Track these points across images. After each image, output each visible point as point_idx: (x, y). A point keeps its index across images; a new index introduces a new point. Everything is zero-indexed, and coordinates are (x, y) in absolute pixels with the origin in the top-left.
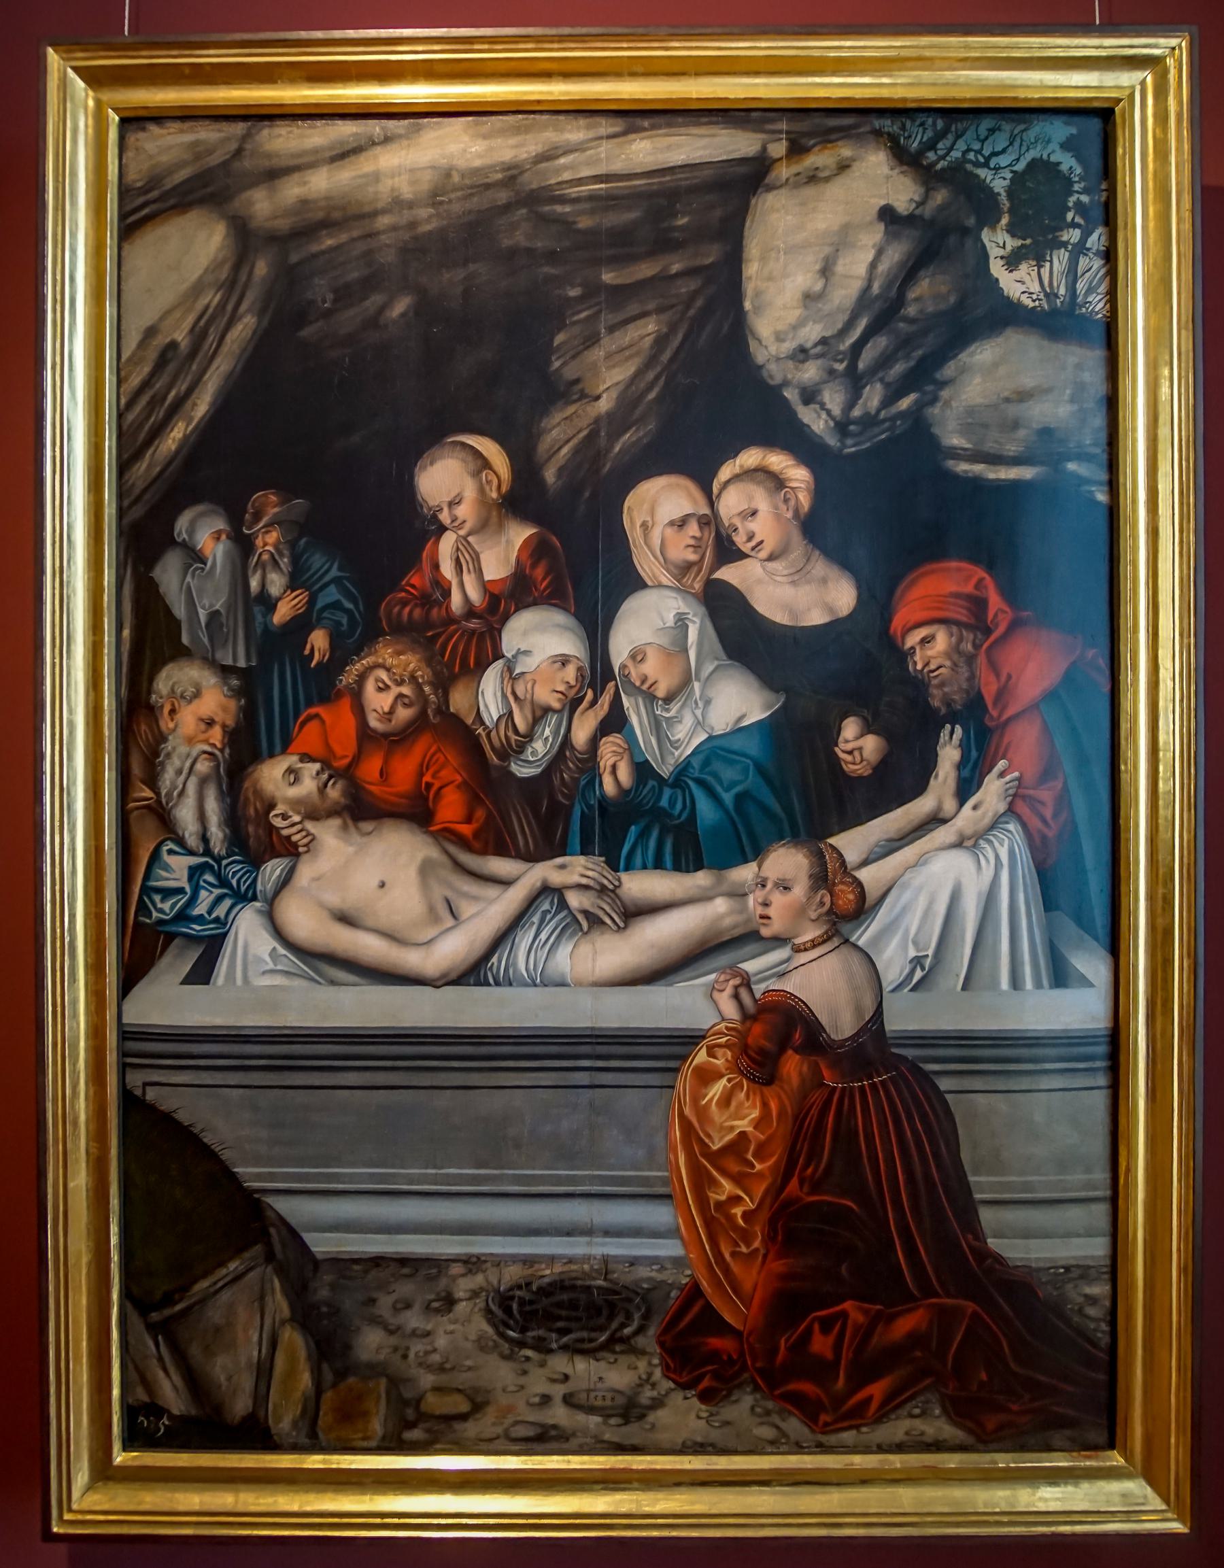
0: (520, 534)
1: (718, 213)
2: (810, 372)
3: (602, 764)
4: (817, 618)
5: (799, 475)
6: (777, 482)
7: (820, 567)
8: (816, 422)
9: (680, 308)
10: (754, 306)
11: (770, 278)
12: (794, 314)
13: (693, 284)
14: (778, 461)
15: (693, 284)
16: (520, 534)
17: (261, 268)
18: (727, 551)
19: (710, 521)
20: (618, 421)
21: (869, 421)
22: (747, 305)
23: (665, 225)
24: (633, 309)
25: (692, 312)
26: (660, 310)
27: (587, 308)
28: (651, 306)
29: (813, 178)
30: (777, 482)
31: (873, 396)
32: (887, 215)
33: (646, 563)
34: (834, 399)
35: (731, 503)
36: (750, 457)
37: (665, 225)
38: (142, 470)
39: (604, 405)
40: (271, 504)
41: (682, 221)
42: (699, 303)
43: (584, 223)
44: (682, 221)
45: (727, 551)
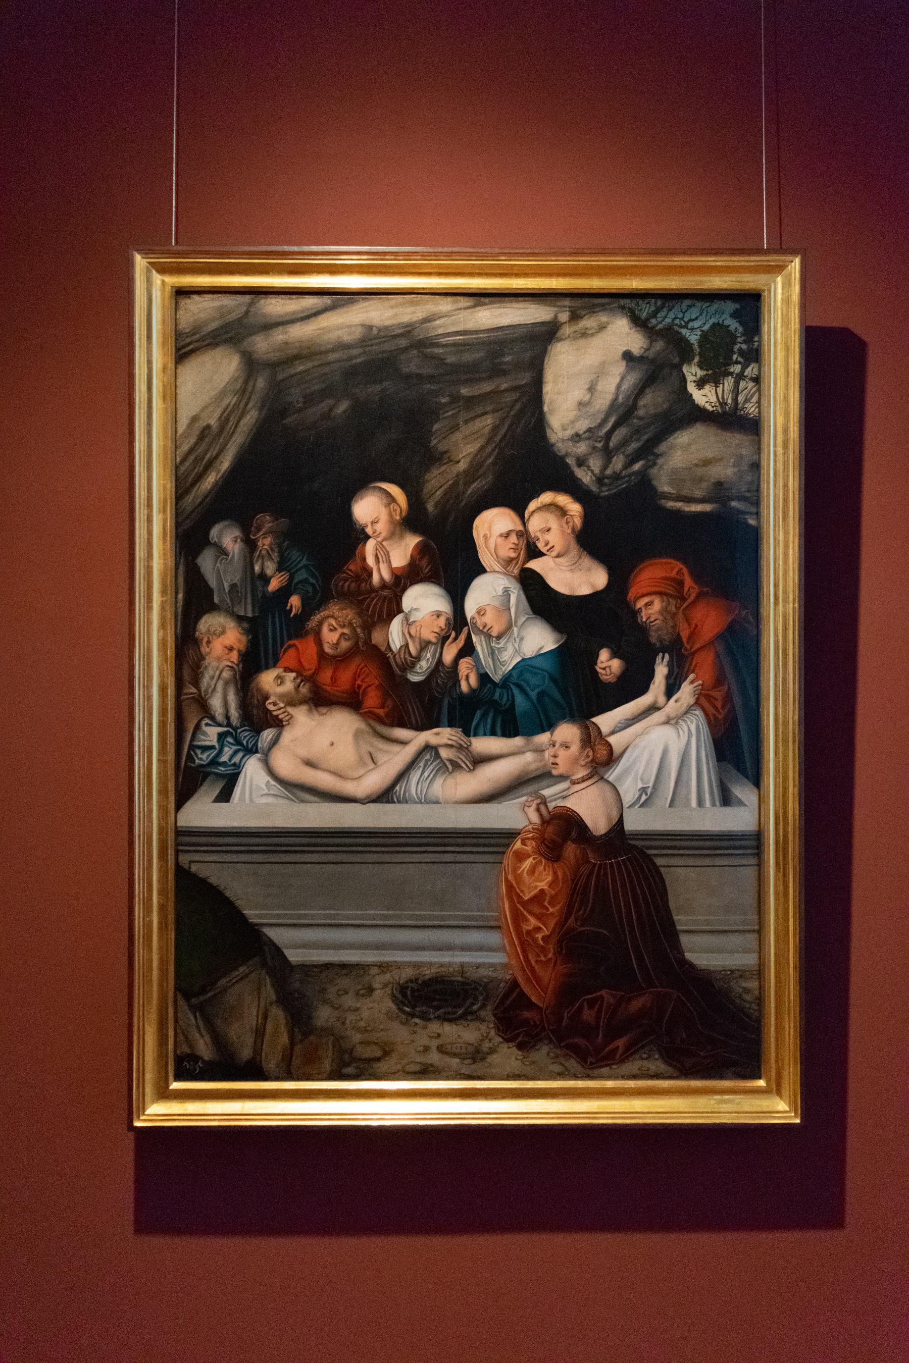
0: (412, 541)
1: (528, 355)
2: (582, 448)
3: (460, 674)
4: (585, 591)
5: (575, 508)
6: (562, 512)
7: (587, 561)
8: (585, 477)
9: (507, 409)
10: (550, 410)
11: (559, 393)
12: (572, 414)
13: (514, 396)
14: (563, 499)
15: (514, 396)
16: (412, 541)
17: (261, 383)
18: (534, 552)
19: (523, 534)
20: (471, 474)
21: (616, 477)
22: (546, 409)
23: (498, 361)
24: (479, 410)
25: (512, 413)
26: (495, 411)
27: (454, 409)
28: (489, 409)
29: (584, 334)
30: (562, 512)
31: (618, 463)
32: (627, 356)
33: (486, 558)
34: (595, 464)
35: (536, 524)
36: (547, 497)
37: (498, 361)
38: (190, 500)
39: (462, 466)
40: (266, 521)
41: (508, 359)
42: (518, 406)
43: (451, 359)
44: (508, 359)
45: (534, 552)
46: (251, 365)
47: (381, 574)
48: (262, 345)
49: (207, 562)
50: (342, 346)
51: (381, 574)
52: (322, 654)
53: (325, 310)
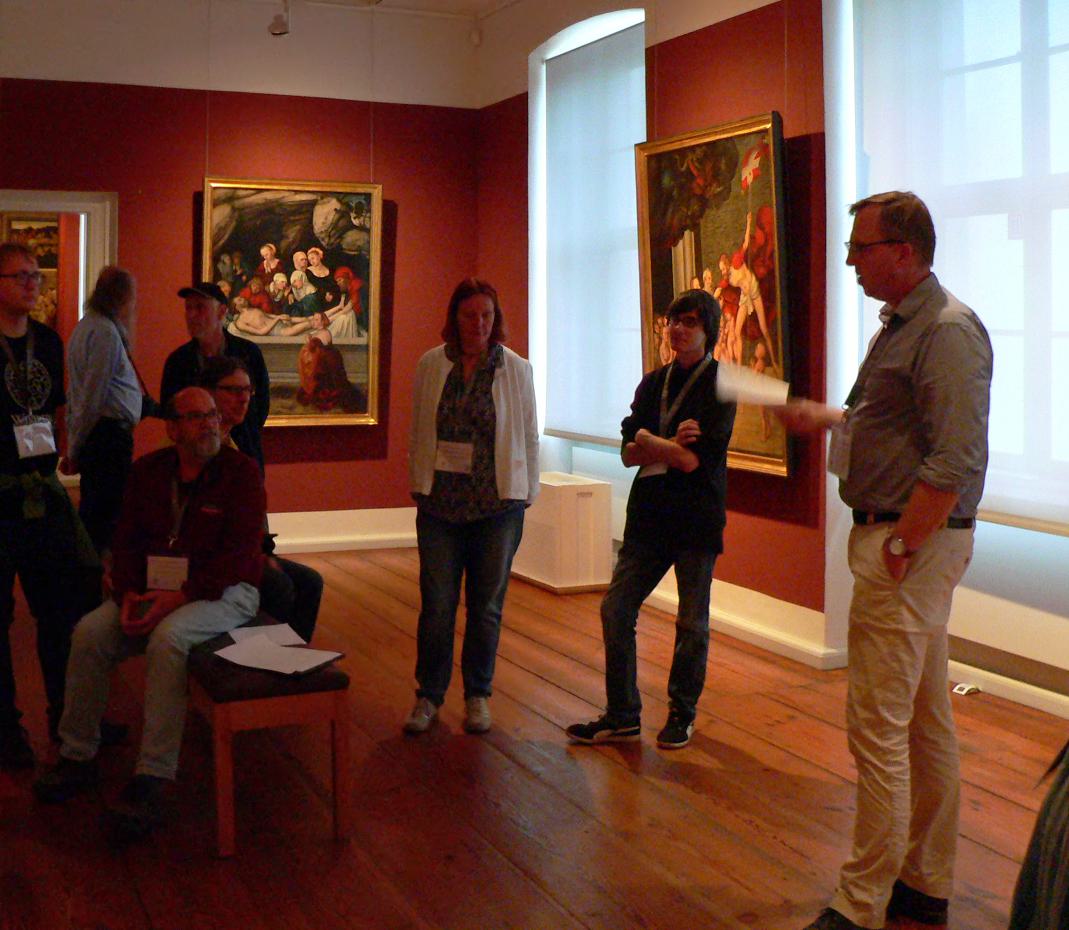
0: (277, 260)
2: (323, 235)
4: (322, 276)
5: (321, 252)
6: (317, 253)
7: (324, 267)
8: (324, 243)
14: (318, 250)
16: (277, 260)
17: (236, 214)
18: (309, 265)
19: (307, 259)
20: (293, 242)
21: (332, 244)
29: (324, 203)
30: (317, 253)
31: (332, 240)
32: (336, 210)
33: (296, 266)
34: (327, 240)
35: (310, 257)
36: (313, 249)
38: (216, 248)
39: (291, 240)
40: (237, 254)
45: (309, 265)
46: (234, 209)
47: (268, 270)
48: (238, 203)
49: (220, 266)
50: (258, 204)
51: (268, 270)
52: (251, 293)
53: (253, 195)
